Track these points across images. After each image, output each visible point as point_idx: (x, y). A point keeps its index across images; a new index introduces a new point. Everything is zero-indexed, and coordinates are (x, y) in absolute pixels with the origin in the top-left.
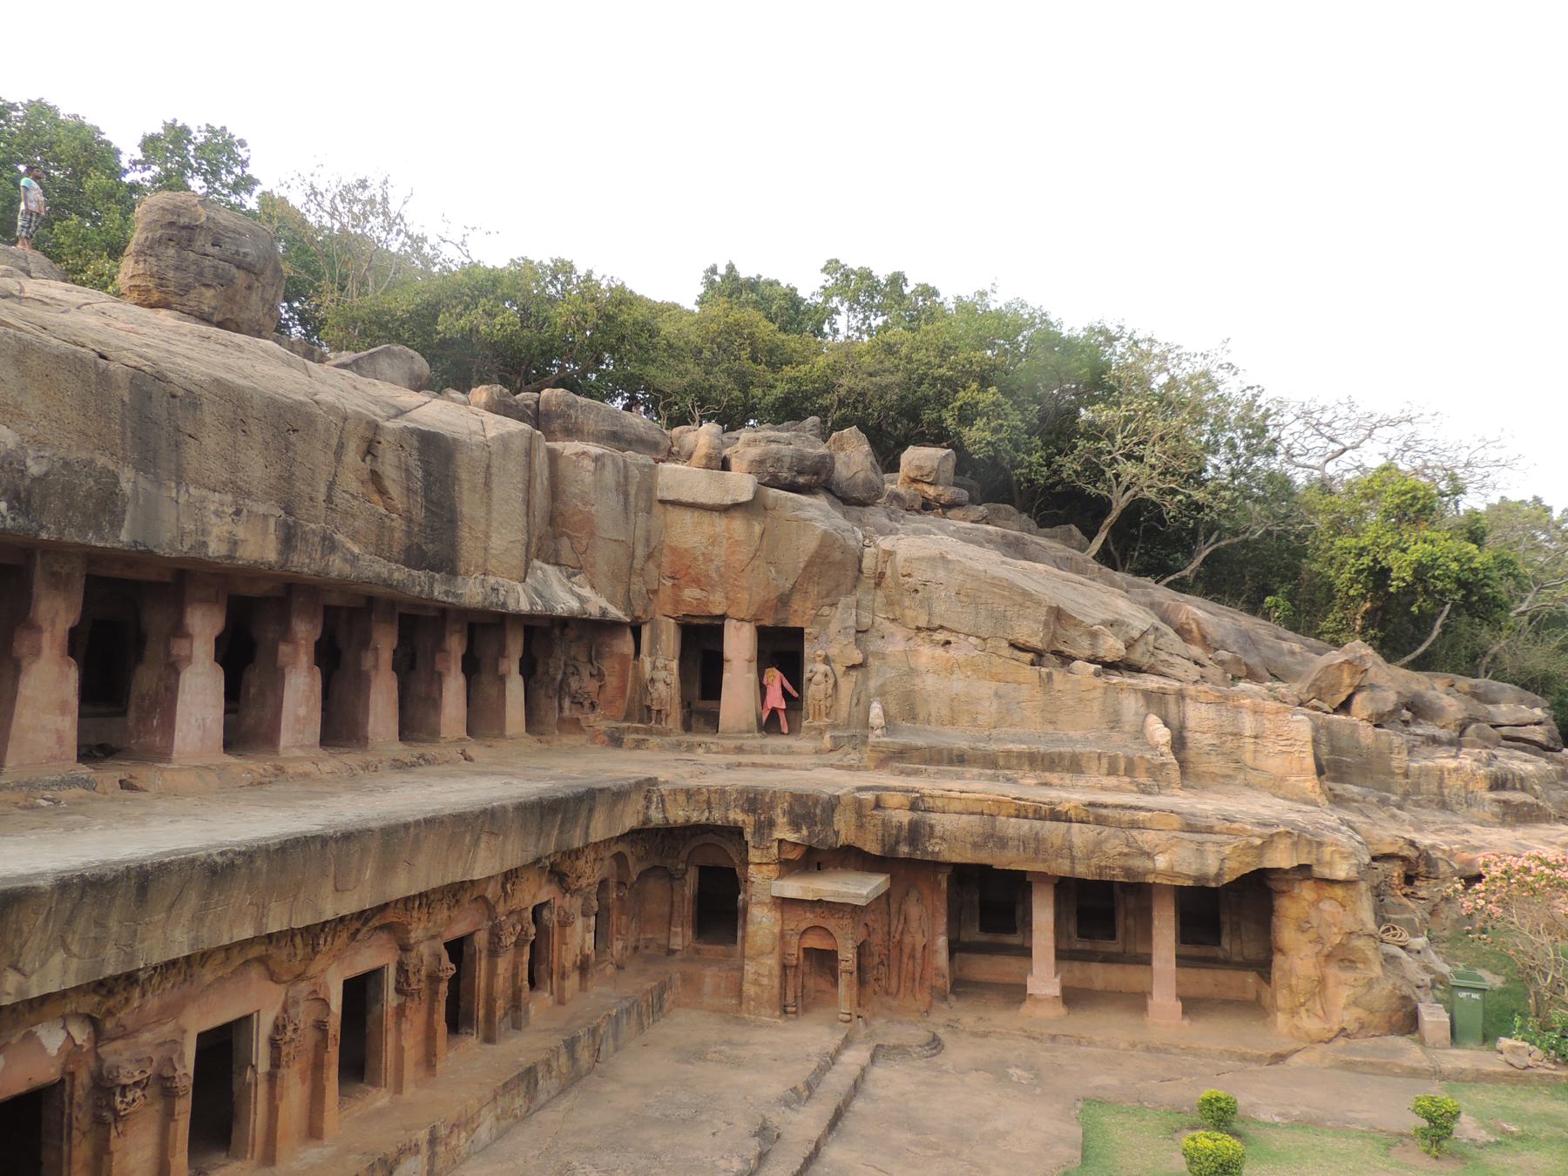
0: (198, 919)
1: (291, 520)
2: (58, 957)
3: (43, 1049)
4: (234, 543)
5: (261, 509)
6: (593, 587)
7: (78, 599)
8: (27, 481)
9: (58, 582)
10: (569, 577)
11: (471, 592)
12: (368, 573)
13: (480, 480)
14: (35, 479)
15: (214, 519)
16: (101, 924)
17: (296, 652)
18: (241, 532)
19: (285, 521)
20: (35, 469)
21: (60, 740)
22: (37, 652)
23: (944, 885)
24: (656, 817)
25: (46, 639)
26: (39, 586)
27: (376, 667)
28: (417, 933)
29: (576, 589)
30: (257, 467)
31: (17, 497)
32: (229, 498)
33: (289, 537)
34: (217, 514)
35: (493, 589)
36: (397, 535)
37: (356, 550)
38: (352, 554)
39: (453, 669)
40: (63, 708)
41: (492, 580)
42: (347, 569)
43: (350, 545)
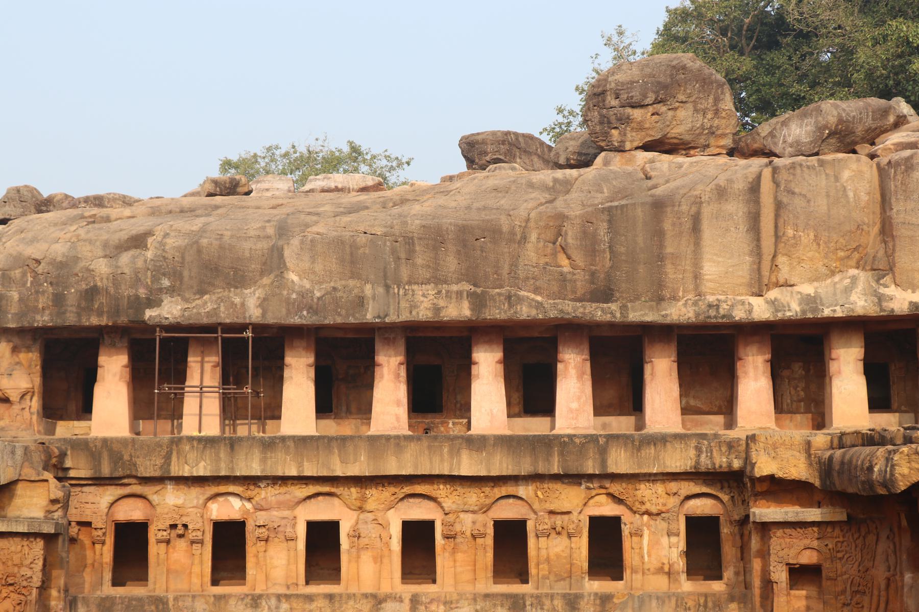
0: (264, 460)
1: (479, 290)
2: (202, 464)
3: (233, 506)
4: (437, 310)
5: (455, 288)
6: (897, 285)
7: (402, 348)
8: (315, 300)
9: (389, 343)
10: (878, 281)
11: (680, 311)
12: (553, 314)
13: (687, 224)
14: (318, 299)
15: (422, 299)
16: (217, 455)
17: (566, 368)
18: (442, 303)
19: (475, 293)
20: (318, 294)
21: (398, 419)
22: (382, 377)
23: (904, 523)
24: (705, 463)
25: (385, 370)
26: (378, 346)
27: (652, 374)
28: (448, 504)
29: (882, 290)
30: (451, 263)
31: (311, 308)
32: (429, 287)
33: (478, 301)
34: (424, 295)
35: (710, 306)
36: (579, 284)
37: (539, 298)
38: (537, 302)
39: (751, 373)
40: (398, 404)
41: (711, 299)
42: (534, 312)
43: (532, 296)
